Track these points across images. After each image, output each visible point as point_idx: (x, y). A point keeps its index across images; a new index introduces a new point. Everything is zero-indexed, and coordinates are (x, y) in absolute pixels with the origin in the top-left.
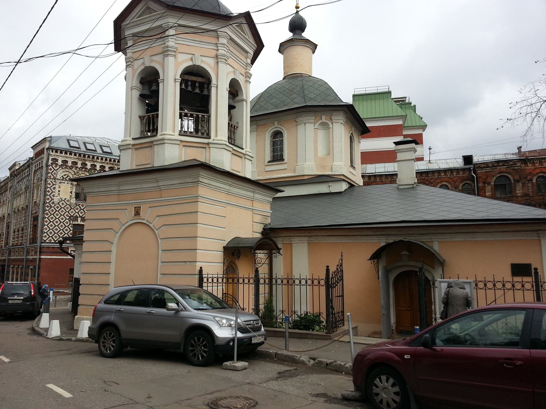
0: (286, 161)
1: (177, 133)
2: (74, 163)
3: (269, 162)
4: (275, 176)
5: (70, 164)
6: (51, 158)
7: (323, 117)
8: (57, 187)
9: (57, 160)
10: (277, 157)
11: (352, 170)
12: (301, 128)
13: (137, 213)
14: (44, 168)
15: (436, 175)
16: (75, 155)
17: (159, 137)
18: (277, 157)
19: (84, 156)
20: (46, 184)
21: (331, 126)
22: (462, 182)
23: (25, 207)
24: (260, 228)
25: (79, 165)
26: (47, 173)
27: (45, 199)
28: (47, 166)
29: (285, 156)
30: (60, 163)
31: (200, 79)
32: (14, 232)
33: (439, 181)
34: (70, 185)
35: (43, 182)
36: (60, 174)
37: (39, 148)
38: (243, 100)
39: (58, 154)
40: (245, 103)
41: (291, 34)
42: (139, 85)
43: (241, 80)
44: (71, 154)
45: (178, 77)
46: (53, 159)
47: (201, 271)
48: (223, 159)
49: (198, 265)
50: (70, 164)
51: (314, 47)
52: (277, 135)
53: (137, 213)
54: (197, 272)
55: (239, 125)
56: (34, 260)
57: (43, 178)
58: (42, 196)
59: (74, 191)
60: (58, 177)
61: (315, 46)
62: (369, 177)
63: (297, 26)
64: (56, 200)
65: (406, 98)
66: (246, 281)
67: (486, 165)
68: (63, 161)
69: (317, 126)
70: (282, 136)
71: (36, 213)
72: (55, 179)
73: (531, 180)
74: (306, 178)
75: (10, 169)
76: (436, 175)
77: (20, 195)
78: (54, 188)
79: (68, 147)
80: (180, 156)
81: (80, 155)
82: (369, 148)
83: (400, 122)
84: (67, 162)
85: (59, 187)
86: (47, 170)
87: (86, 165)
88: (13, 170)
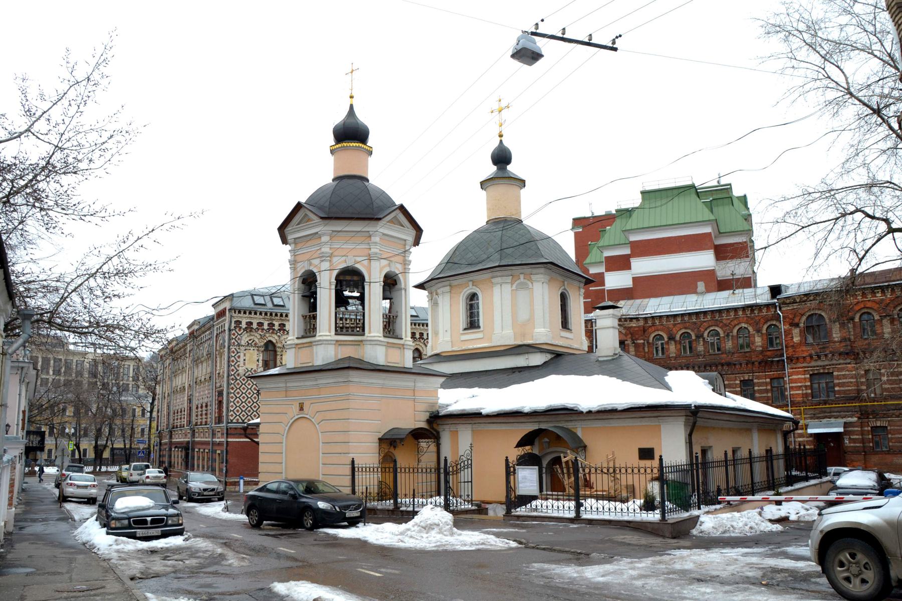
0: (482, 329)
1: (333, 332)
2: (260, 324)
3: (465, 329)
4: (471, 347)
5: (255, 326)
6: (233, 320)
7: (522, 276)
8: (242, 355)
9: (240, 322)
10: (473, 324)
11: (565, 334)
12: (496, 290)
13: (301, 409)
14: (227, 332)
15: (732, 314)
16: (261, 314)
17: (317, 338)
18: (473, 324)
19: (271, 314)
20: (229, 353)
21: (530, 286)
22: (766, 322)
23: (207, 378)
24: (426, 416)
25: (266, 327)
26: (230, 339)
27: (228, 371)
28: (230, 330)
29: (481, 324)
30: (244, 325)
31: (355, 278)
32: (197, 408)
33: (736, 322)
34: (256, 352)
35: (226, 349)
36: (245, 338)
37: (221, 308)
38: (401, 289)
39: (242, 314)
40: (403, 292)
41: (495, 168)
42: (302, 286)
43: (397, 269)
44: (256, 313)
45: (333, 280)
46: (236, 322)
47: (353, 462)
48: (378, 355)
49: (352, 456)
50: (255, 326)
51: (522, 183)
52: (473, 297)
53: (301, 409)
54: (349, 462)
55: (399, 314)
56: (220, 444)
57: (226, 344)
58: (226, 366)
59: (261, 358)
60: (243, 343)
61: (523, 182)
62: (646, 318)
63: (502, 158)
64: (241, 370)
65: (730, 185)
66: (407, 470)
67: (792, 300)
68: (247, 323)
69: (514, 286)
70: (478, 299)
71: (221, 386)
72: (239, 345)
73: (852, 319)
74: (502, 349)
75: (189, 328)
76: (732, 314)
77: (202, 362)
78: (239, 357)
79: (253, 306)
80: (336, 355)
81: (266, 314)
82: (665, 269)
83: (707, 230)
84: (251, 323)
85: (245, 355)
86: (230, 335)
87: (274, 325)
88: (191, 330)
